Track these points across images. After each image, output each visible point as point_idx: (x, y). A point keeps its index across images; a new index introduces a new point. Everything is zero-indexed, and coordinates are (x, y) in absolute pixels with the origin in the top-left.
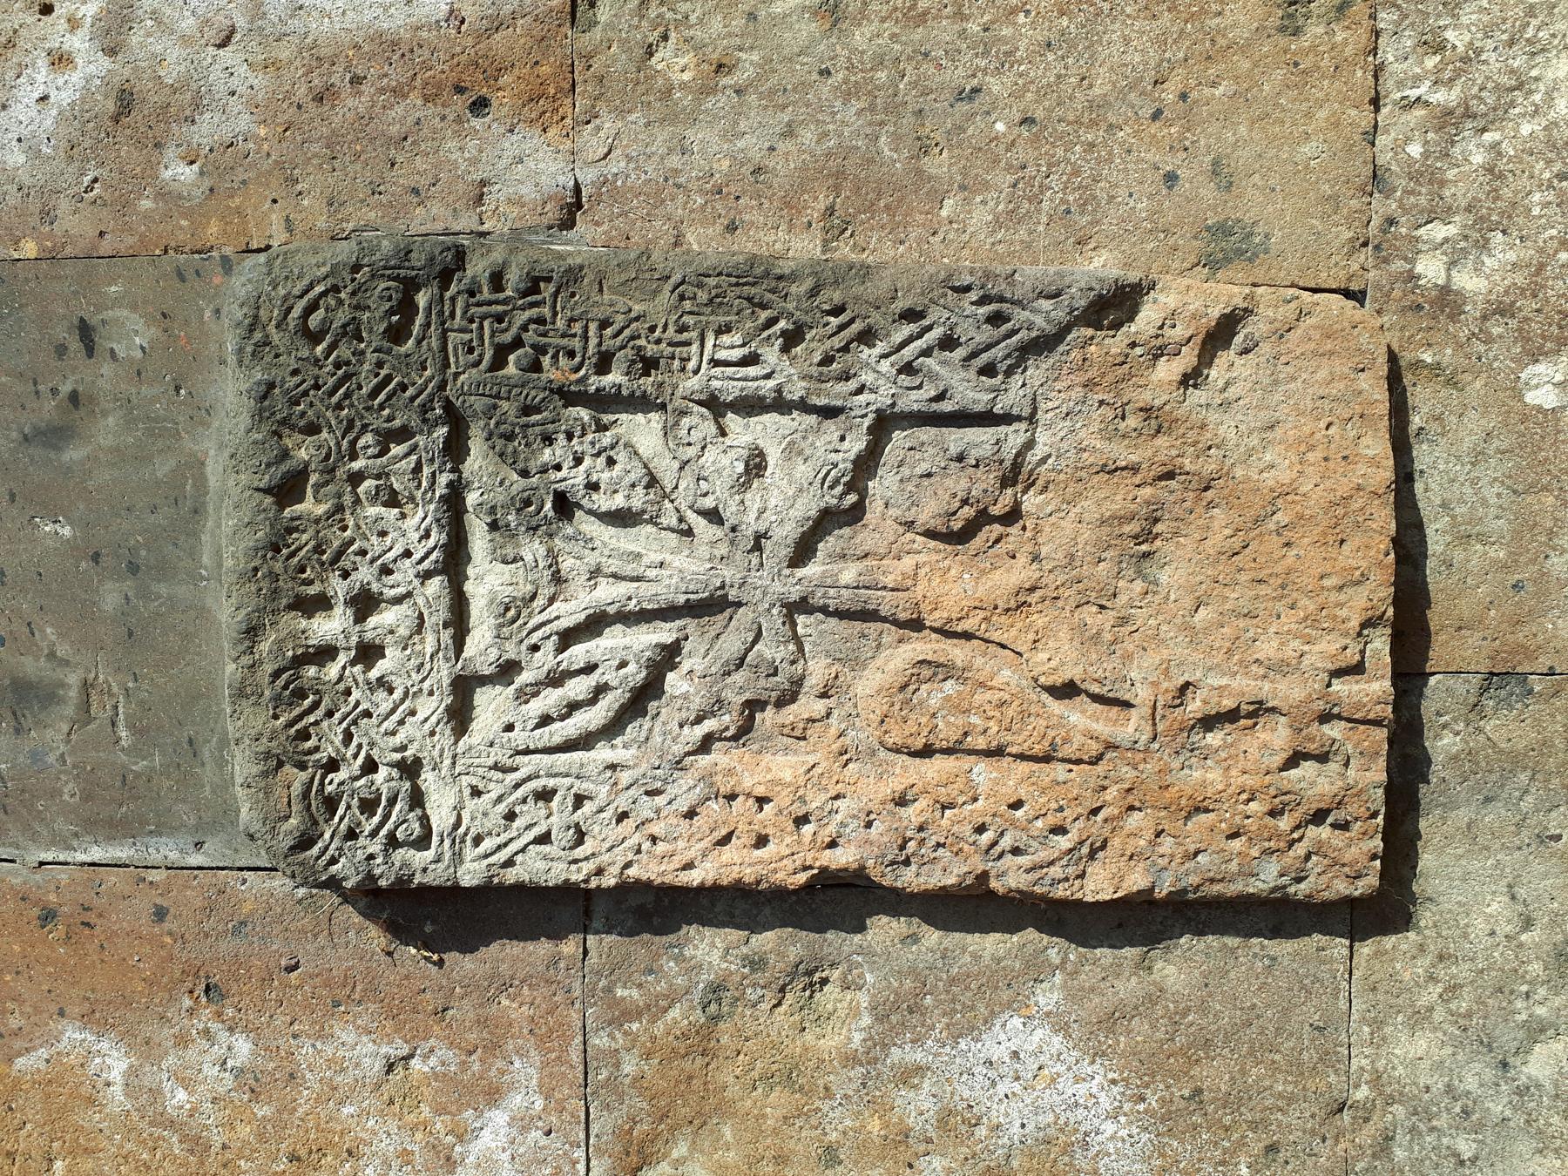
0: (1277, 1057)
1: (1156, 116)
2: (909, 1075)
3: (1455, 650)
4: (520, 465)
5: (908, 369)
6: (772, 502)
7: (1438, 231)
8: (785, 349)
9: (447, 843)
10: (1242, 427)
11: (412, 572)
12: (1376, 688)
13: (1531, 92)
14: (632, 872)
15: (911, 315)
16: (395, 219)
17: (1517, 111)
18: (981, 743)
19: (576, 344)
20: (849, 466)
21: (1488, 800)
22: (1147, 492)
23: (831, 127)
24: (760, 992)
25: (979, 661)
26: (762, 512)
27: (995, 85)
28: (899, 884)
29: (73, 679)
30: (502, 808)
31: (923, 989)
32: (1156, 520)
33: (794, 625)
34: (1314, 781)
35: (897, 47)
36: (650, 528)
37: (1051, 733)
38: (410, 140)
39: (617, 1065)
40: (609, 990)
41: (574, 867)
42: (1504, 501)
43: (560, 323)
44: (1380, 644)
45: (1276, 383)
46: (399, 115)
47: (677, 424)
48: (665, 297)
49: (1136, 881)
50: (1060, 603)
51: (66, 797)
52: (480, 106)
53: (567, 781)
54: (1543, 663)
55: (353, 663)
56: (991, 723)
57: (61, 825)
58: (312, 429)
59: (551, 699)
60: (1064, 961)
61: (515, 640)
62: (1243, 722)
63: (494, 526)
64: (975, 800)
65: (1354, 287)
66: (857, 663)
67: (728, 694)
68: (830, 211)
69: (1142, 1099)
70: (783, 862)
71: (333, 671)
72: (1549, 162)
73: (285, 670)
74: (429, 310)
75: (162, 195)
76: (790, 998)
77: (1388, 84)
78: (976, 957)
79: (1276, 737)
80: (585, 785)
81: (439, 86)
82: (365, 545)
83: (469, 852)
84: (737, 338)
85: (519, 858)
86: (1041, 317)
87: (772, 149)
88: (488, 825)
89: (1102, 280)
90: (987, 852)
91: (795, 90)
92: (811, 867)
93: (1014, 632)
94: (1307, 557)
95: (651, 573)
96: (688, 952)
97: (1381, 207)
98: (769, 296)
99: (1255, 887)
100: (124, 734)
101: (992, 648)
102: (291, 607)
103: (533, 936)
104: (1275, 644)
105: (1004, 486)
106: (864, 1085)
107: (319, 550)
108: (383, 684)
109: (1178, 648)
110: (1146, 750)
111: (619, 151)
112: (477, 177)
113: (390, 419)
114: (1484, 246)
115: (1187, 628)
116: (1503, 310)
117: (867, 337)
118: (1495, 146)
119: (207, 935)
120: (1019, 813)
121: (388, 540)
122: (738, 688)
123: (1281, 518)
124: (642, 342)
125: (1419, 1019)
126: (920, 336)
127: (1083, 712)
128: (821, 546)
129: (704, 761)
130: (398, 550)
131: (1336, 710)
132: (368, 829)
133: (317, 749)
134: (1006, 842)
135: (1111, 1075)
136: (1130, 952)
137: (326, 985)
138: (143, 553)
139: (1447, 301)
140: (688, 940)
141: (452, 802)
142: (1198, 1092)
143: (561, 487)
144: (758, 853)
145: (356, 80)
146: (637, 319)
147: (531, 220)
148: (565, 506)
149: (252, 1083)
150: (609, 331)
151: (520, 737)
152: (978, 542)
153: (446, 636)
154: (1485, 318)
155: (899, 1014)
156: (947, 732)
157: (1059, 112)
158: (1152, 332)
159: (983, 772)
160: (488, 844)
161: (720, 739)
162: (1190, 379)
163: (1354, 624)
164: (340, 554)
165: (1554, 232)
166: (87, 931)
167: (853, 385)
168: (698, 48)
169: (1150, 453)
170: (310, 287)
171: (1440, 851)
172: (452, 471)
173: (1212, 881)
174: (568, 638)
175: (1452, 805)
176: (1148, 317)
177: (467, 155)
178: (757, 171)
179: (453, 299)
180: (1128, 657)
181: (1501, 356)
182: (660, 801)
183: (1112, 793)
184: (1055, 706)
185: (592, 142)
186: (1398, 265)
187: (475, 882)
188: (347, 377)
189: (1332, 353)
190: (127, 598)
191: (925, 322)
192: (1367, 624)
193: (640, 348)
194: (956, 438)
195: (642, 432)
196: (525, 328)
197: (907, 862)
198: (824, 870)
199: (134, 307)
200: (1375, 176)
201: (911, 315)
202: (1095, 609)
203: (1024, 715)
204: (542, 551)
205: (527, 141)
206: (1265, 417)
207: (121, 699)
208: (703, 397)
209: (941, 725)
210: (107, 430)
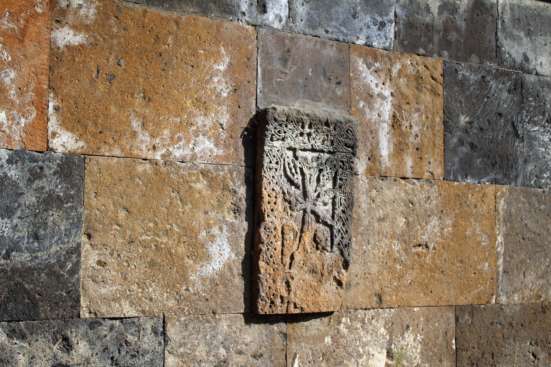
1: (365, 273)
2: (221, 229)
5: (339, 231)
7: (349, 320)
15: (347, 231)
21: (267, 336)
27: (370, 247)
29: (287, 71)
31: (235, 232)
34: (278, 301)
40: (235, 170)
46: (369, 145)
48: (350, 191)
49: (262, 271)
54: (288, 343)
58: (335, 129)
59: (292, 165)
66: (295, 221)
71: (300, 128)
75: (359, 101)
76: (233, 206)
77: (367, 311)
78: (241, 243)
79: (285, 294)
83: (269, 148)
86: (346, 253)
94: (310, 298)
97: (352, 311)
99: (261, 291)
102: (311, 122)
103: (245, 156)
108: (297, 136)
109: (298, 278)
114: (347, 328)
122: (292, 199)
134: (269, 247)
139: (340, 322)
142: (217, 285)
145: (373, 138)
148: (321, 171)
149: (218, 95)
151: (287, 159)
152: (313, 243)
153: (303, 148)
156: (286, 237)
159: (280, 243)
160: (270, 152)
162: (335, 277)
164: (317, 131)
174: (301, 169)
176: (343, 271)
183: (277, 266)
185: (364, 178)
186: (344, 314)
194: (329, 239)
198: (264, 214)
199: (343, 93)
201: (347, 231)
205: (365, 167)
206: (328, 291)
210: (325, 85)
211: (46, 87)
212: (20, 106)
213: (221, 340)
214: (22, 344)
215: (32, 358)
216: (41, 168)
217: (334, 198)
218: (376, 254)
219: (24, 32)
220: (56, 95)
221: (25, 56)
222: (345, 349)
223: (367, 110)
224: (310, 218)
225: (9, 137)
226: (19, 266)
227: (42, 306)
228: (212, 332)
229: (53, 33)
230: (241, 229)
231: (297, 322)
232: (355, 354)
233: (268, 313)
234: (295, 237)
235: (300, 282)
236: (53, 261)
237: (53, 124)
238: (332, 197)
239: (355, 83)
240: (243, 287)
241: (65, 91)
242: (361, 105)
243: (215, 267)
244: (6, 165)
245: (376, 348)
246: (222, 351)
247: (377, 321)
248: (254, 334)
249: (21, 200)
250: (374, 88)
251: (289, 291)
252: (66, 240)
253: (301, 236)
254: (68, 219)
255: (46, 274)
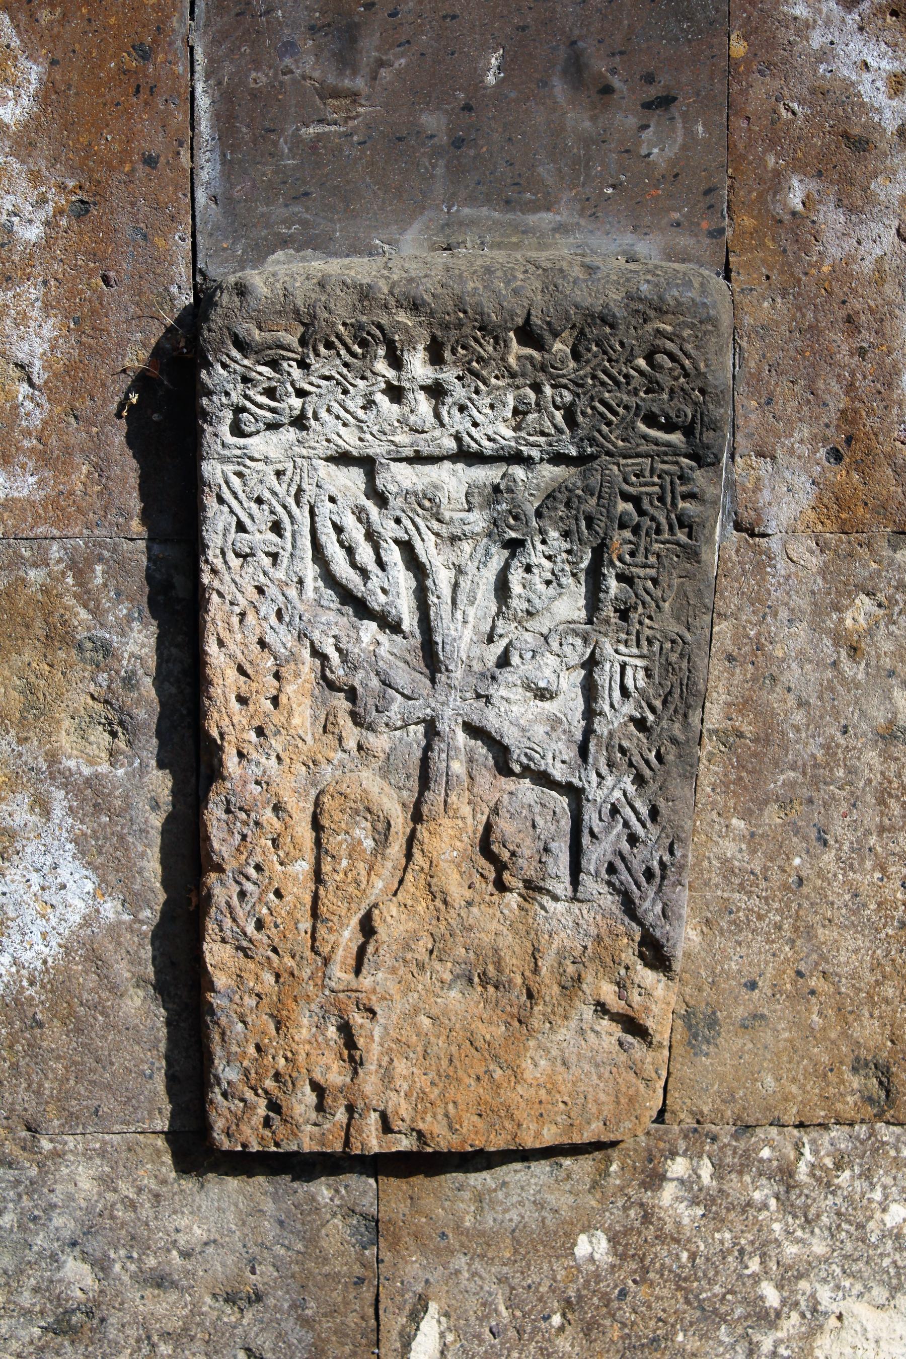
0: (72, 1082)
1: (799, 974)
2: (42, 805)
3: (395, 1196)
4: (545, 512)
5: (615, 811)
6: (515, 708)
7: (706, 1171)
8: (632, 719)
9: (238, 452)
10: (565, 1044)
11: (460, 428)
12: (372, 1140)
13: (803, 1229)
14: (215, 597)
16: (748, 384)
17: (790, 1220)
18: (326, 868)
19: (640, 559)
20: (543, 768)
21: (281, 1223)
22: (519, 980)
23: (804, 735)
24: (104, 684)
25: (389, 865)
26: (508, 700)
27: (828, 858)
28: (211, 805)
30: (267, 495)
32: (497, 987)
33: (416, 724)
35: (862, 784)
36: (494, 609)
37: (335, 919)
38: (811, 397)
39: (35, 565)
40: (100, 559)
41: (218, 551)
42: (506, 1224)
43: (656, 547)
44: (405, 1144)
45: (597, 1066)
47: (577, 635)
49: (221, 980)
50: (434, 922)
51: (254, 75)
52: (836, 455)
53: (289, 547)
54: (386, 1255)
55: (388, 383)
56: (342, 875)
57: (228, 68)
58: (576, 355)
59: (356, 532)
60: (142, 922)
61: (405, 506)
62: (346, 1052)
63: (496, 489)
64: (281, 864)
65: (667, 1116)
66: (385, 772)
67: (361, 674)
68: (740, 735)
69: (32, 983)
70: (226, 718)
71: (381, 366)
72: (752, 1243)
73: (384, 335)
74: (668, 444)
76: (98, 707)
78: (143, 855)
79: (335, 1075)
80: (285, 561)
81: (853, 422)
82: (483, 394)
83: (230, 468)
84: (641, 684)
85: (225, 509)
87: (789, 690)
88: (251, 483)
89: (674, 946)
90: (241, 873)
91: (834, 707)
92: (222, 738)
93: (413, 890)
94: (469, 1091)
95: (459, 615)
96: (136, 625)
98: (672, 707)
99: (219, 1064)
100: (311, 130)
101: (399, 874)
102: (434, 338)
103: (143, 497)
104: (405, 1072)
105: (525, 881)
106: (32, 769)
107: (480, 359)
109: (400, 1005)
110: (323, 986)
111: (793, 569)
112: (779, 453)
113: (583, 413)
115: (416, 1011)
116: (647, 1218)
117: (640, 780)
118: (765, 1206)
119: (133, 204)
120: (272, 896)
121: (488, 411)
122: (366, 681)
123: (498, 1074)
124: (640, 610)
125: (106, 1182)
126: (639, 820)
127: (351, 940)
128: (479, 743)
129: (306, 653)
130: (479, 418)
131: (356, 1116)
132: (250, 393)
133: (317, 354)
134: (249, 887)
135: (50, 960)
136: (150, 971)
137: (93, 312)
138: (472, 152)
140: (146, 626)
141: (272, 455)
142: (40, 1025)
143: (529, 545)
144: (233, 699)
145: (862, 352)
146: (658, 606)
147: (742, 497)
148: (514, 546)
150: (649, 584)
151: (325, 509)
152: (482, 861)
153: (409, 452)
154: (642, 1205)
155: (92, 797)
156: (333, 842)
157: (806, 904)
158: (636, 981)
159: (303, 867)
160: (236, 482)
161: (323, 666)
162: (601, 1008)
163: (421, 1126)
164: (477, 375)
165: (702, 1248)
166: (131, 90)
167: (604, 770)
168: (870, 632)
169: (547, 981)
170: (688, 356)
171: (241, 1192)
172: (542, 460)
173: (223, 1034)
174: (407, 547)
175: (276, 1198)
176: (647, 976)
177: (796, 445)
178: (773, 679)
179: (677, 463)
180: (393, 971)
181: (614, 1216)
182: (273, 620)
183: (289, 962)
184: (355, 920)
186: (682, 1145)
187: (206, 475)
188: (617, 383)
189: (618, 1103)
190: (432, 137)
191: (649, 824)
192: (420, 1134)
193: (636, 609)
195: (571, 605)
196: (653, 519)
197: (228, 811)
198: (221, 748)
199: (684, 147)
200: (748, 1127)
201: (654, 813)
202: (430, 946)
203: (350, 899)
204: (477, 529)
206: (573, 1059)
207: (343, 129)
208: (597, 656)
209: (339, 838)
210: (578, 120)
213: (66, 1234)
217: (591, 663)
218: (864, 890)
222: (679, 1288)
223: (831, 218)
224: (459, 753)
228: (26, 1202)
230: (142, 804)
231: (427, 1176)
232: (739, 1311)
233: (255, 1147)
234: (383, 836)
235: (414, 1025)
238: (574, 659)
239: (760, 90)
240: (163, 1032)
242: (795, 199)
243: (27, 956)
245: (859, 1287)
246: (77, 1274)
247: (867, 1175)
248: (213, 1216)
250: (882, 99)
251: (355, 1063)
253: (411, 839)
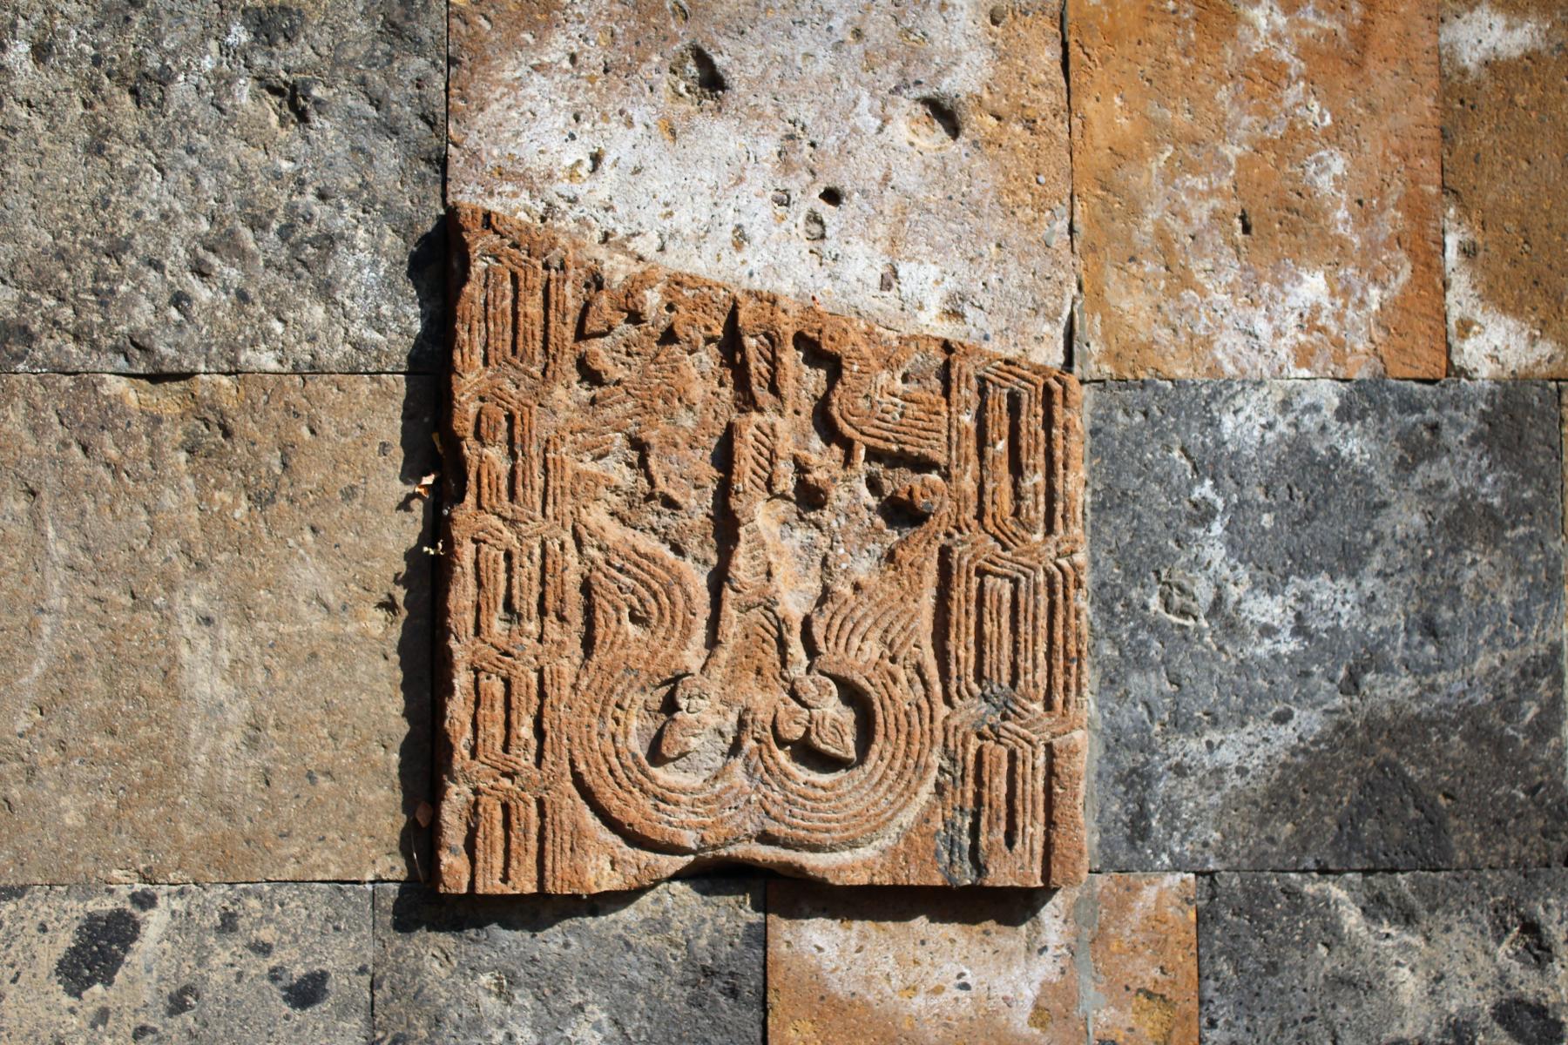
211: (1433, 190)
212: (1362, 249)
214: (1407, 938)
215: (1437, 980)
216: (1434, 428)
219: (1362, 37)
220: (1465, 210)
221: (1369, 106)
225: (1339, 344)
226: (1387, 714)
227: (1458, 829)
229: (1445, 29)
236: (1482, 698)
237: (1461, 298)
241: (1491, 196)
244: (1334, 425)
249: (1383, 523)
252: (1517, 637)
254: (1519, 572)
255: (1464, 737)
